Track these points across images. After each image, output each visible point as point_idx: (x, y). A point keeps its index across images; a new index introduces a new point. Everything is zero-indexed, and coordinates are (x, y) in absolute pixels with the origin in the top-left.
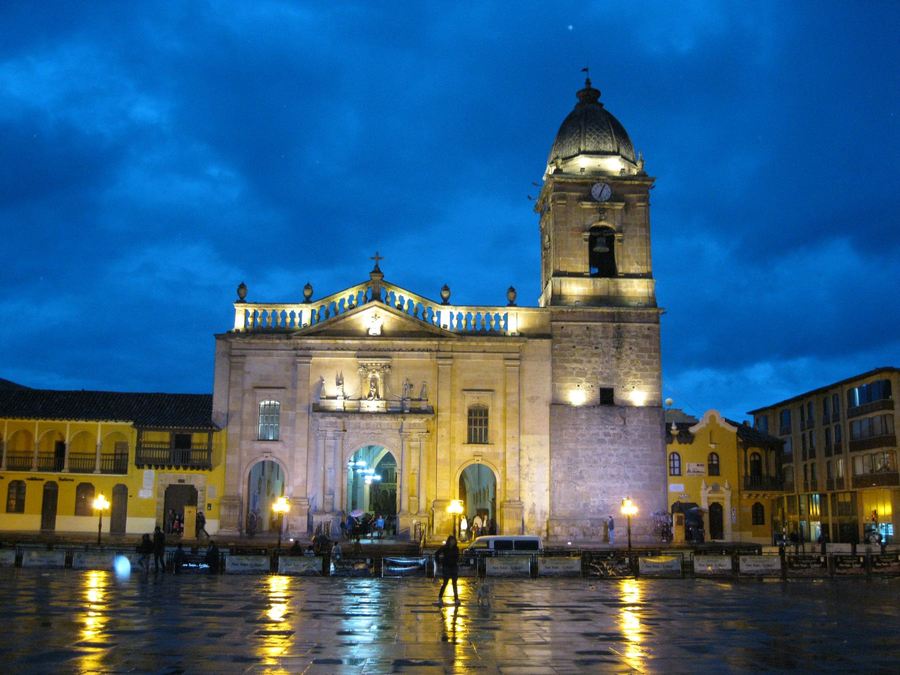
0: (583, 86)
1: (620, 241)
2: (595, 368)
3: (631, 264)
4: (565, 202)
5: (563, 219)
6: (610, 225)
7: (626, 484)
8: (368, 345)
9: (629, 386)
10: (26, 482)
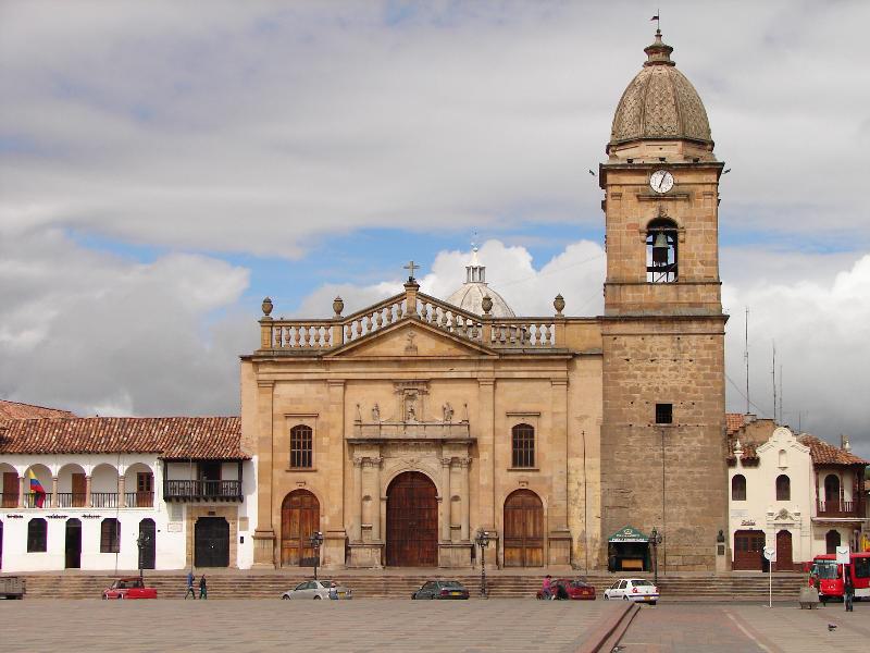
0: (652, 41)
5: (617, 215)
7: (683, 510)
10: (47, 519)
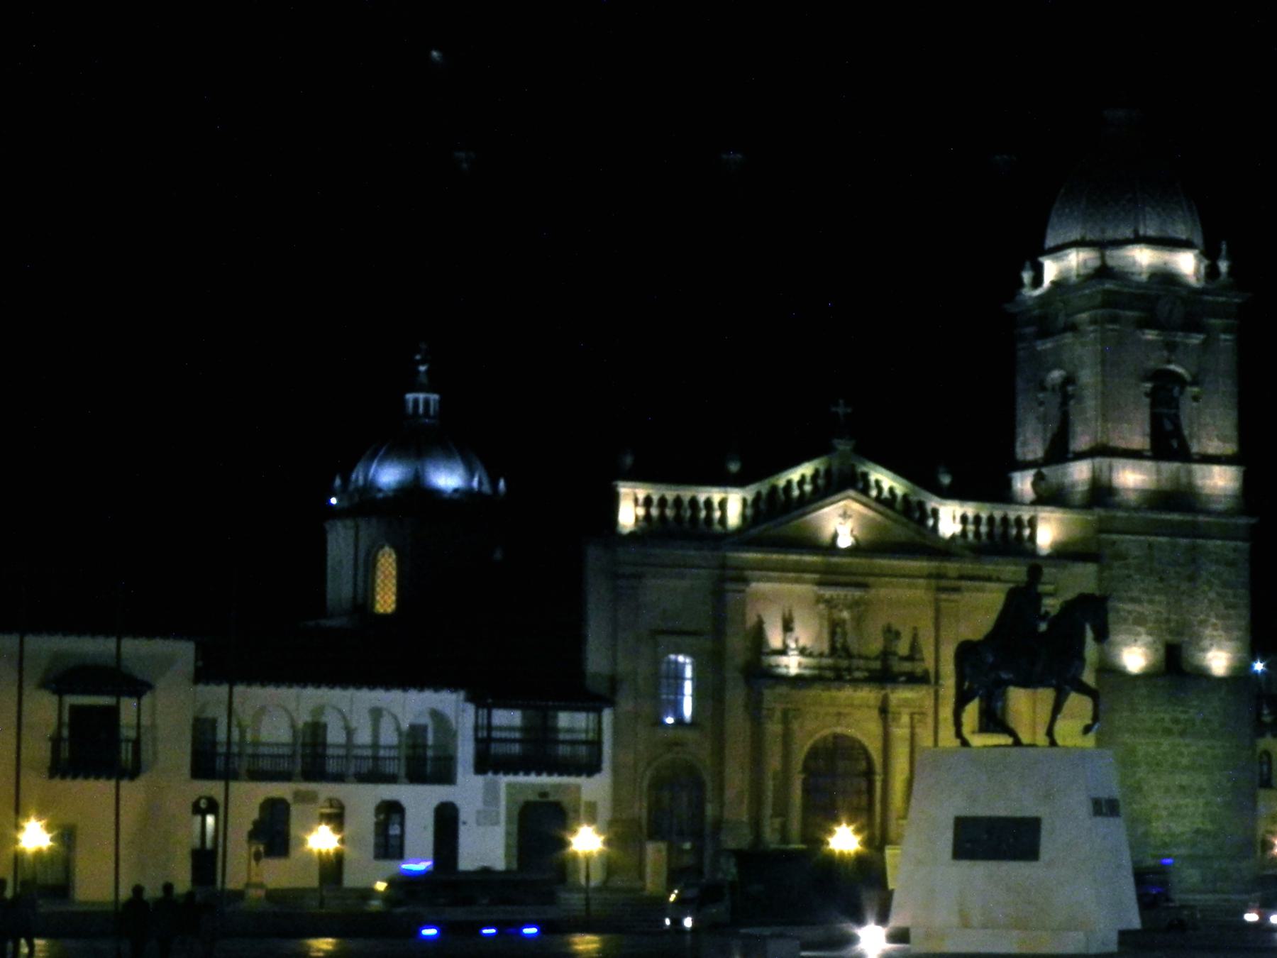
1: (1196, 398)
2: (1158, 612)
4: (1116, 327)
6: (1180, 370)
7: (1201, 802)
8: (837, 565)
9: (1206, 643)
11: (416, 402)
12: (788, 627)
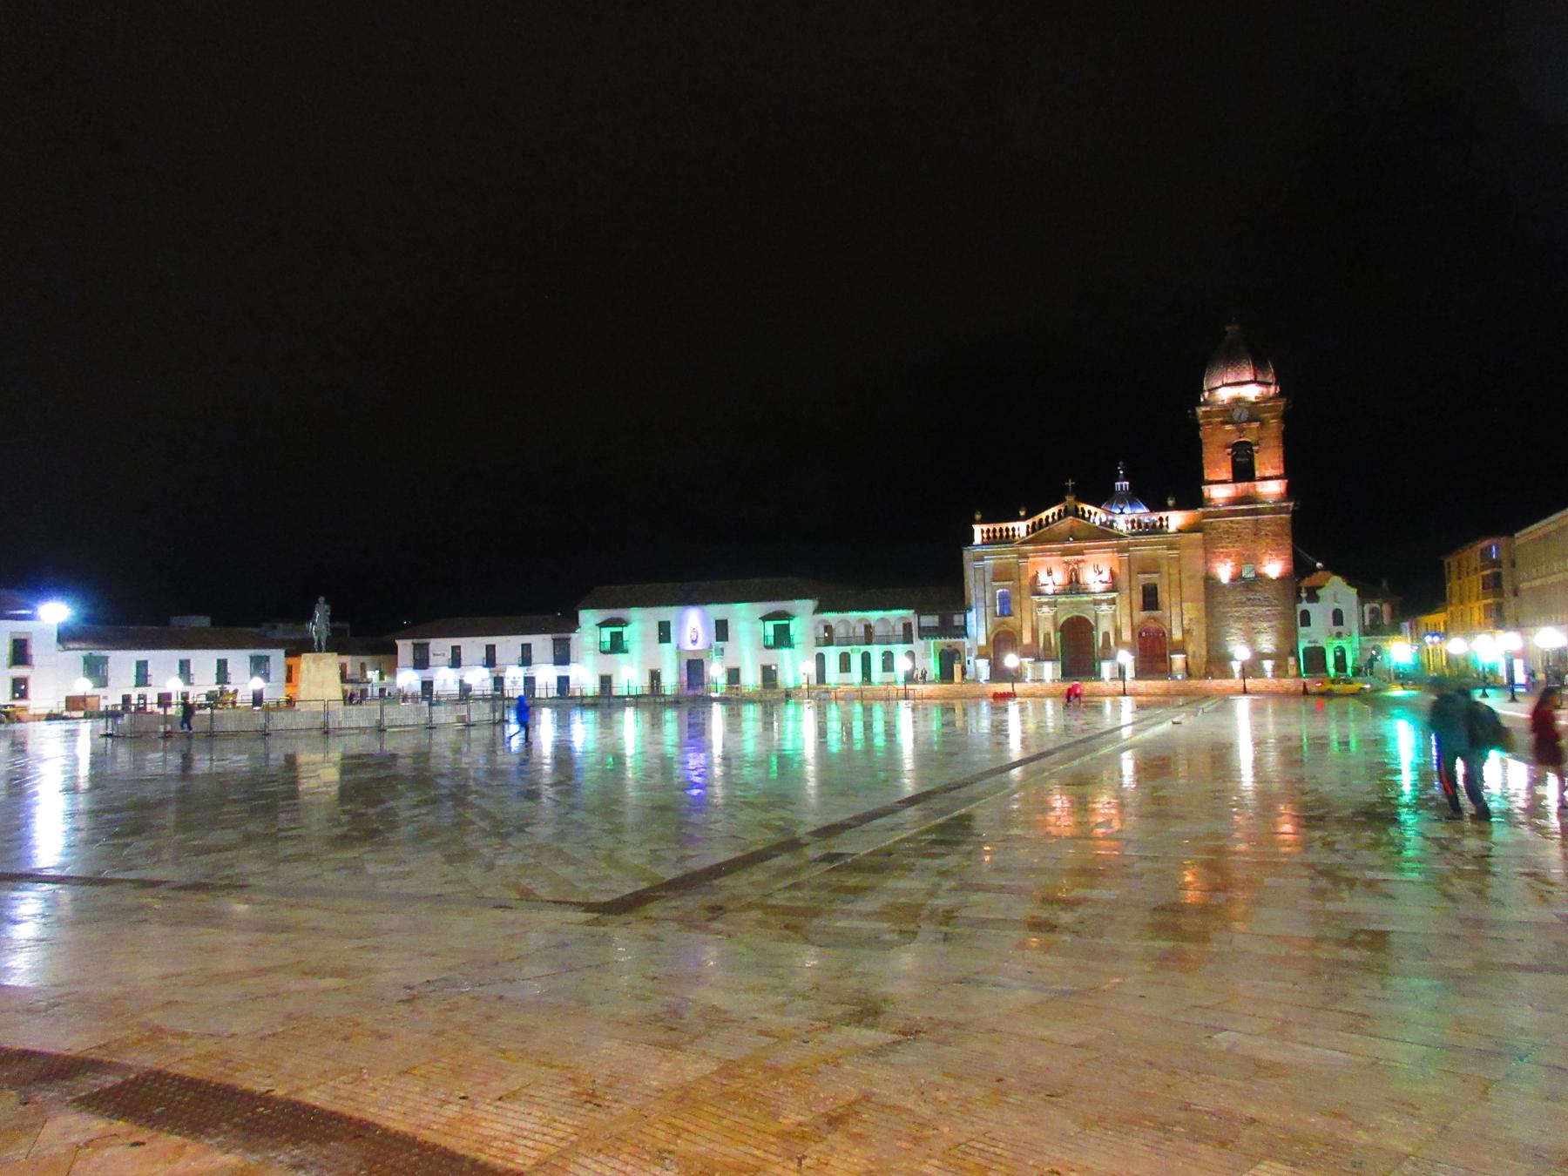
1: (1257, 452)
3: (1266, 469)
11: (1122, 486)
12: (1050, 573)
